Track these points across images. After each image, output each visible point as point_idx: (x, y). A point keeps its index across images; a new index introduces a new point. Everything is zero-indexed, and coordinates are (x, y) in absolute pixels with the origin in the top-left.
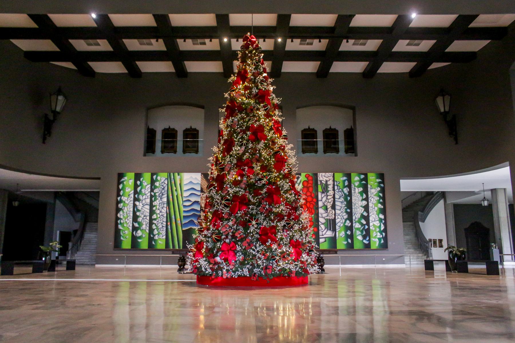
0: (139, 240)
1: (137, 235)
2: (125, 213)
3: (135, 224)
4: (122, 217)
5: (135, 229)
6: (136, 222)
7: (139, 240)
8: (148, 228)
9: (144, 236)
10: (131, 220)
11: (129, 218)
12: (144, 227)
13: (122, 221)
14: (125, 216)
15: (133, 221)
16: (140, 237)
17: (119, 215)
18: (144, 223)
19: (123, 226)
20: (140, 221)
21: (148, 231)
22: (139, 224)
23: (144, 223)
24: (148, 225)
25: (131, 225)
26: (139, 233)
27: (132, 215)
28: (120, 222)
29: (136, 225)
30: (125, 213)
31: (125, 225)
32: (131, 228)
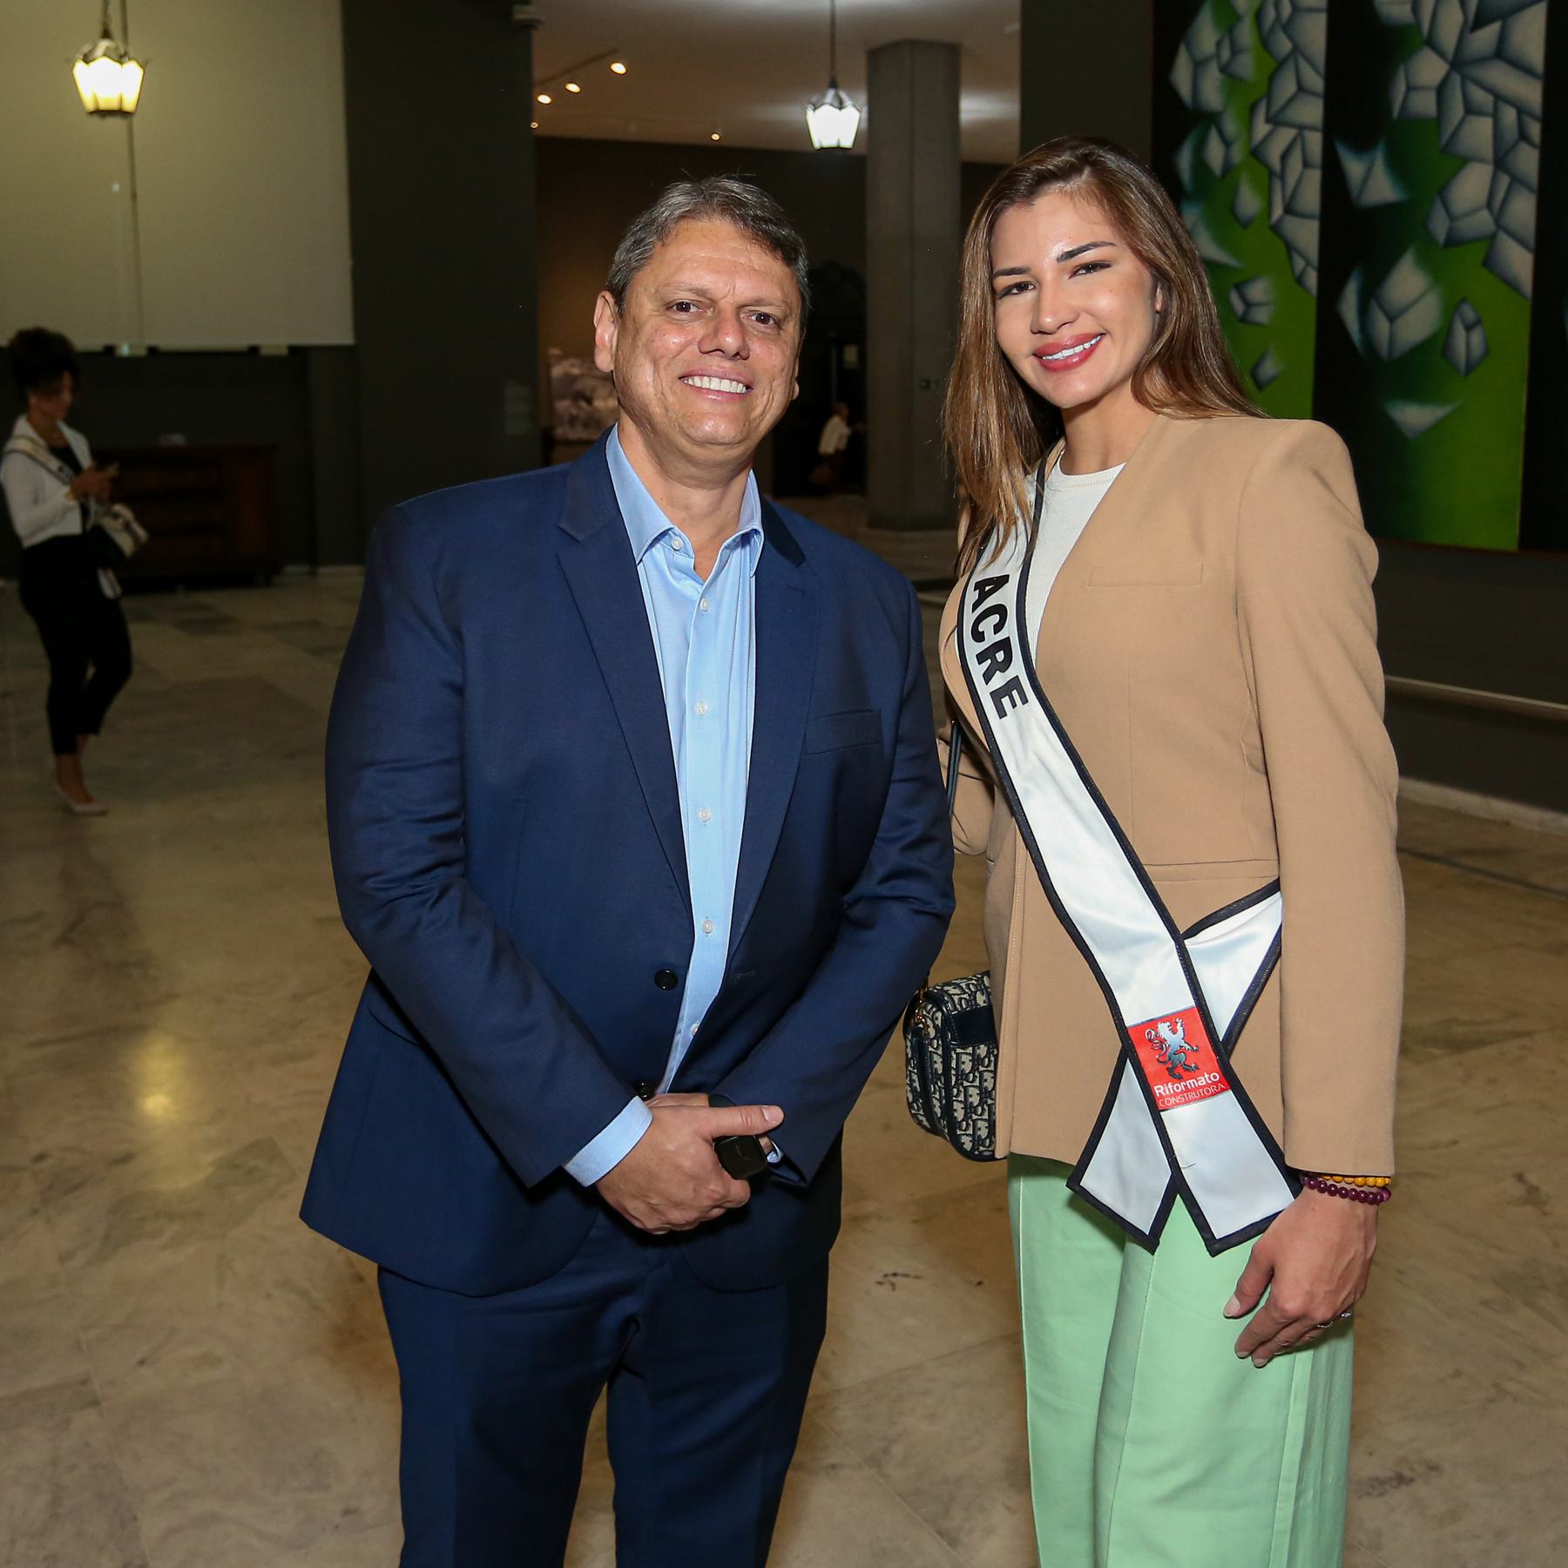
0: (1413, 416)
1: (1381, 326)
2: (1246, 34)
3: (1354, 167)
4: (1212, 94)
5: (1358, 243)
6: (1362, 146)
7: (1413, 416)
8: (1523, 209)
9: (1465, 343)
10: (1312, 112)
11: (1287, 86)
12: (1471, 186)
13: (1215, 153)
14: (1247, 65)
15: (1333, 128)
16: (1420, 369)
17: (1182, 76)
18: (1479, 134)
19: (1227, 220)
20: (1425, 104)
21: (1520, 262)
22: (1400, 168)
23: (1479, 134)
24: (1528, 161)
25: (1311, 197)
26: (1412, 299)
27: (1315, 32)
28: (1200, 164)
29: (1374, 181)
30: (1246, 34)
31: (1249, 202)
32: (1307, 235)
